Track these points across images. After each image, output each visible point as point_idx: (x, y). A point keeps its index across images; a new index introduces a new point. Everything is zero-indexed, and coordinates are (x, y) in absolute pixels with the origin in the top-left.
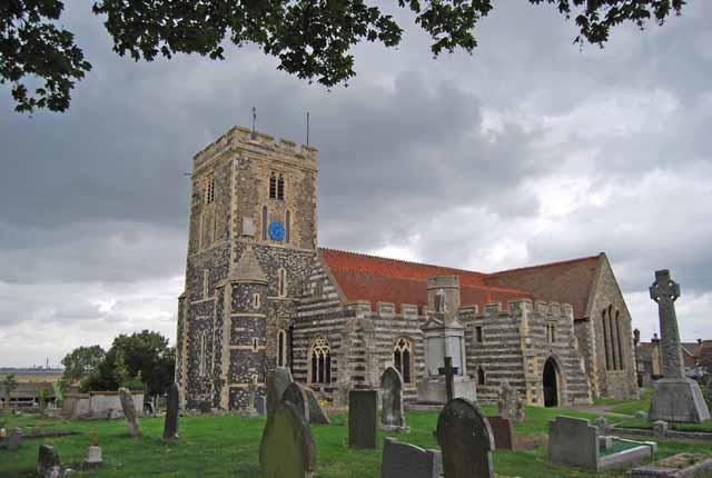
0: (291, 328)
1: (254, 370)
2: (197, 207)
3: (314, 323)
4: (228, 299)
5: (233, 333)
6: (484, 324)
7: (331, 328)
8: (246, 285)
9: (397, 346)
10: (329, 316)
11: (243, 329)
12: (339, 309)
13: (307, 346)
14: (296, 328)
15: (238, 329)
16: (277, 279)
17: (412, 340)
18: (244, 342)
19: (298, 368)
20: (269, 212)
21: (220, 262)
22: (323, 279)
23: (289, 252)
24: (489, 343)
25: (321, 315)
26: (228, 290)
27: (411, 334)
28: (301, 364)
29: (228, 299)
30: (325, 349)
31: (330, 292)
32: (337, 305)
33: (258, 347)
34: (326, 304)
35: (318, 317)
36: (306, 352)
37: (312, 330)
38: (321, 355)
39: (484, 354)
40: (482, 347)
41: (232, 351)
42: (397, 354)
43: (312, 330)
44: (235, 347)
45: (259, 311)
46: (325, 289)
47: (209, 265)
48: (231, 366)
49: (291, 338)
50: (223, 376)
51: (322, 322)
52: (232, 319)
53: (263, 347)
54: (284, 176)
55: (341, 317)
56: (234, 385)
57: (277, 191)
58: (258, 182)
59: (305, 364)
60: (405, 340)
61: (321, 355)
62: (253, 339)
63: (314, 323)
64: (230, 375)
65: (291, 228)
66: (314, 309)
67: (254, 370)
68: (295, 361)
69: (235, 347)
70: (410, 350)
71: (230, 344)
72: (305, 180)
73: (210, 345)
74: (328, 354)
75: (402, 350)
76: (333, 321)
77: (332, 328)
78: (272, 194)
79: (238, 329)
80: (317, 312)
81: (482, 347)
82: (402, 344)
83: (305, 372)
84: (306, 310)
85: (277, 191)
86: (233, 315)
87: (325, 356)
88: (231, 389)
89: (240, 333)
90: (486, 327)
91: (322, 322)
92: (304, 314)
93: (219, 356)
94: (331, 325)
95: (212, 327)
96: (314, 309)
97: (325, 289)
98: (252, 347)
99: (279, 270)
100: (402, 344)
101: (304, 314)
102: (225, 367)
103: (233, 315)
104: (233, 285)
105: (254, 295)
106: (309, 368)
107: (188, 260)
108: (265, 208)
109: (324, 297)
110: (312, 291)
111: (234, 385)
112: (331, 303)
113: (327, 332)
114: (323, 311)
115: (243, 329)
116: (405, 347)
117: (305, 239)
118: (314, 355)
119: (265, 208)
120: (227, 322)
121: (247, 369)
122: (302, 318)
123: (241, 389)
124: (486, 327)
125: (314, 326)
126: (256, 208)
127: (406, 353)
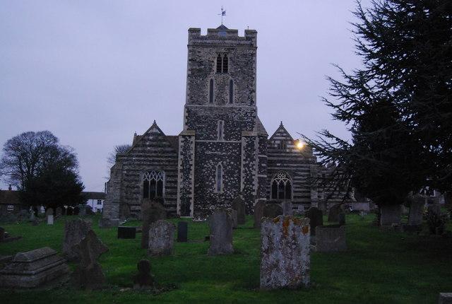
2: (200, 71)
4: (257, 146)
7: (293, 169)
12: (299, 159)
26: (257, 139)
29: (257, 146)
30: (285, 180)
35: (280, 161)
37: (276, 168)
38: (282, 183)
43: (276, 168)
50: (254, 194)
51: (285, 165)
52: (259, 158)
61: (282, 183)
71: (258, 173)
74: (288, 183)
77: (295, 169)
80: (283, 159)
87: (285, 184)
91: (285, 165)
94: (293, 167)
97: (288, 146)
104: (259, 137)
107: (186, 107)
109: (288, 151)
114: (288, 159)
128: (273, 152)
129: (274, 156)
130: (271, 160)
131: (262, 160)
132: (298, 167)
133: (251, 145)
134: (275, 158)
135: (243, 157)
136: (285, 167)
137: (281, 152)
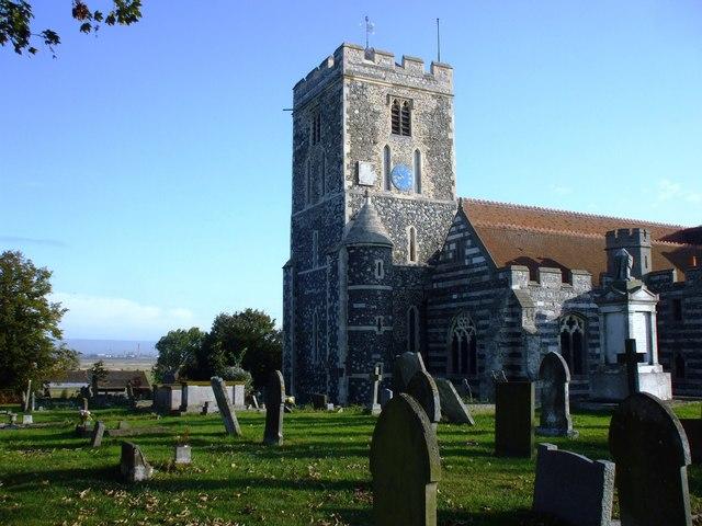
0: (425, 303)
1: (379, 356)
3: (455, 296)
5: (352, 312)
6: (685, 296)
7: (476, 303)
8: (366, 248)
9: (565, 327)
10: (472, 288)
11: (363, 305)
12: (486, 278)
13: (446, 326)
14: (431, 304)
15: (355, 306)
16: (406, 240)
17: (586, 319)
18: (366, 322)
19: (435, 354)
20: (393, 153)
21: (332, 220)
22: (464, 239)
23: (419, 204)
24: (691, 321)
25: (464, 286)
26: (343, 255)
27: (582, 309)
28: (438, 350)
31: (475, 255)
32: (484, 273)
33: (383, 329)
34: (469, 271)
35: (458, 289)
36: (445, 334)
37: (453, 305)
38: (464, 338)
39: (685, 336)
40: (683, 327)
41: (350, 333)
42: (565, 336)
43: (453, 305)
44: (353, 328)
45: (382, 282)
46: (468, 252)
47: (318, 224)
48: (350, 352)
49: (424, 317)
51: (464, 295)
53: (389, 328)
54: (415, 103)
55: (489, 288)
56: (354, 376)
57: (401, 124)
58: (376, 114)
59: (444, 349)
60: (575, 318)
61: (464, 338)
62: (377, 318)
63: (455, 296)
64: (348, 363)
65: (423, 173)
66: (456, 278)
67: (379, 356)
68: (431, 345)
69: (353, 328)
70: (582, 331)
72: (437, 108)
73: (323, 325)
74: (473, 337)
75: (572, 332)
76: (478, 294)
78: (396, 130)
79: (355, 306)
80: (457, 282)
81: (683, 327)
82: (571, 323)
83: (445, 359)
84: (443, 280)
85: (401, 124)
86: (350, 288)
87: (469, 339)
88: (351, 380)
89: (359, 311)
90: (688, 300)
91: (464, 295)
92: (441, 285)
93: (334, 339)
95: (325, 304)
96: (456, 278)
97: (468, 252)
98: (376, 328)
99: (408, 229)
100: (571, 323)
101: (441, 285)
102: (342, 354)
103: (350, 288)
104: (349, 249)
105: (377, 262)
106: (448, 354)
108: (387, 147)
110: (451, 256)
111: (354, 376)
112: (476, 270)
113: (471, 308)
114: (466, 281)
115: (363, 305)
116: (575, 327)
117: (439, 187)
118: (455, 338)
119: (387, 147)
120: (343, 297)
121: (369, 355)
122: (438, 289)
123: (364, 380)
124: (688, 300)
125: (455, 301)
126: (375, 149)
127: (577, 333)
128: (448, 271)
129: (448, 279)
130: (445, 289)
131: (354, 296)
132: (482, 297)
133: (335, 269)
134: (450, 284)
135: (329, 295)
136: (463, 300)
137: (458, 269)
